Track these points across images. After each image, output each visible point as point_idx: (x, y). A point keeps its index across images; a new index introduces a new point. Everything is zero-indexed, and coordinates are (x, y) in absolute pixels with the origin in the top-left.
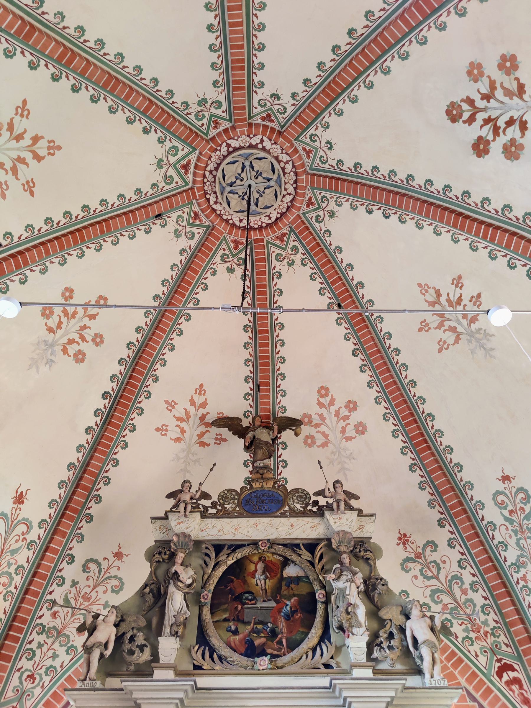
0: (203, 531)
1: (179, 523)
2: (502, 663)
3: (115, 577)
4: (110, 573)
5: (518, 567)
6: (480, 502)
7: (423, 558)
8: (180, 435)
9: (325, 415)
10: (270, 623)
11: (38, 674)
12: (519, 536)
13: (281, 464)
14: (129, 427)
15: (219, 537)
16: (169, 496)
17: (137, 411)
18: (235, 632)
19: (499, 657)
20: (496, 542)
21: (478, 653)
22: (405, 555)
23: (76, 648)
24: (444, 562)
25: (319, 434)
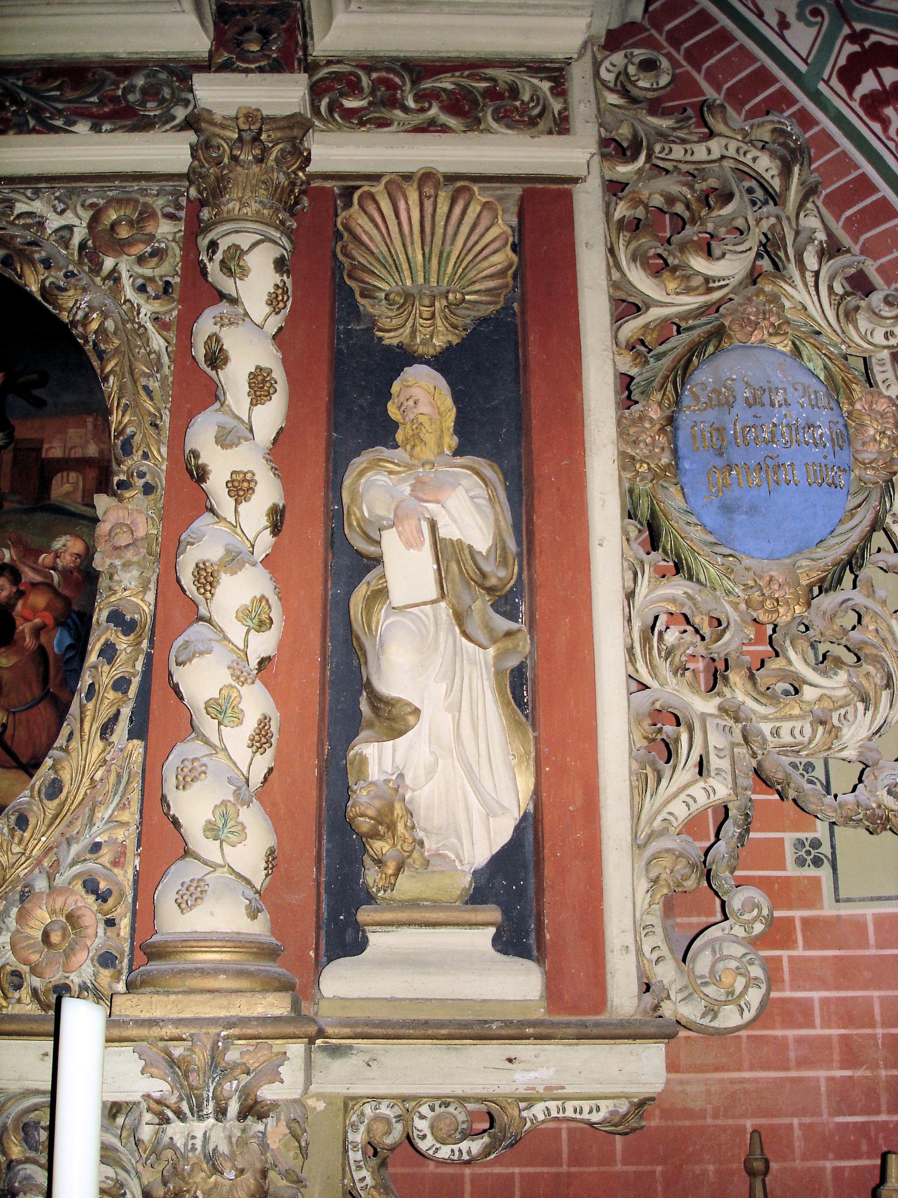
2: (867, 44)
19: (858, 27)
21: (791, 18)
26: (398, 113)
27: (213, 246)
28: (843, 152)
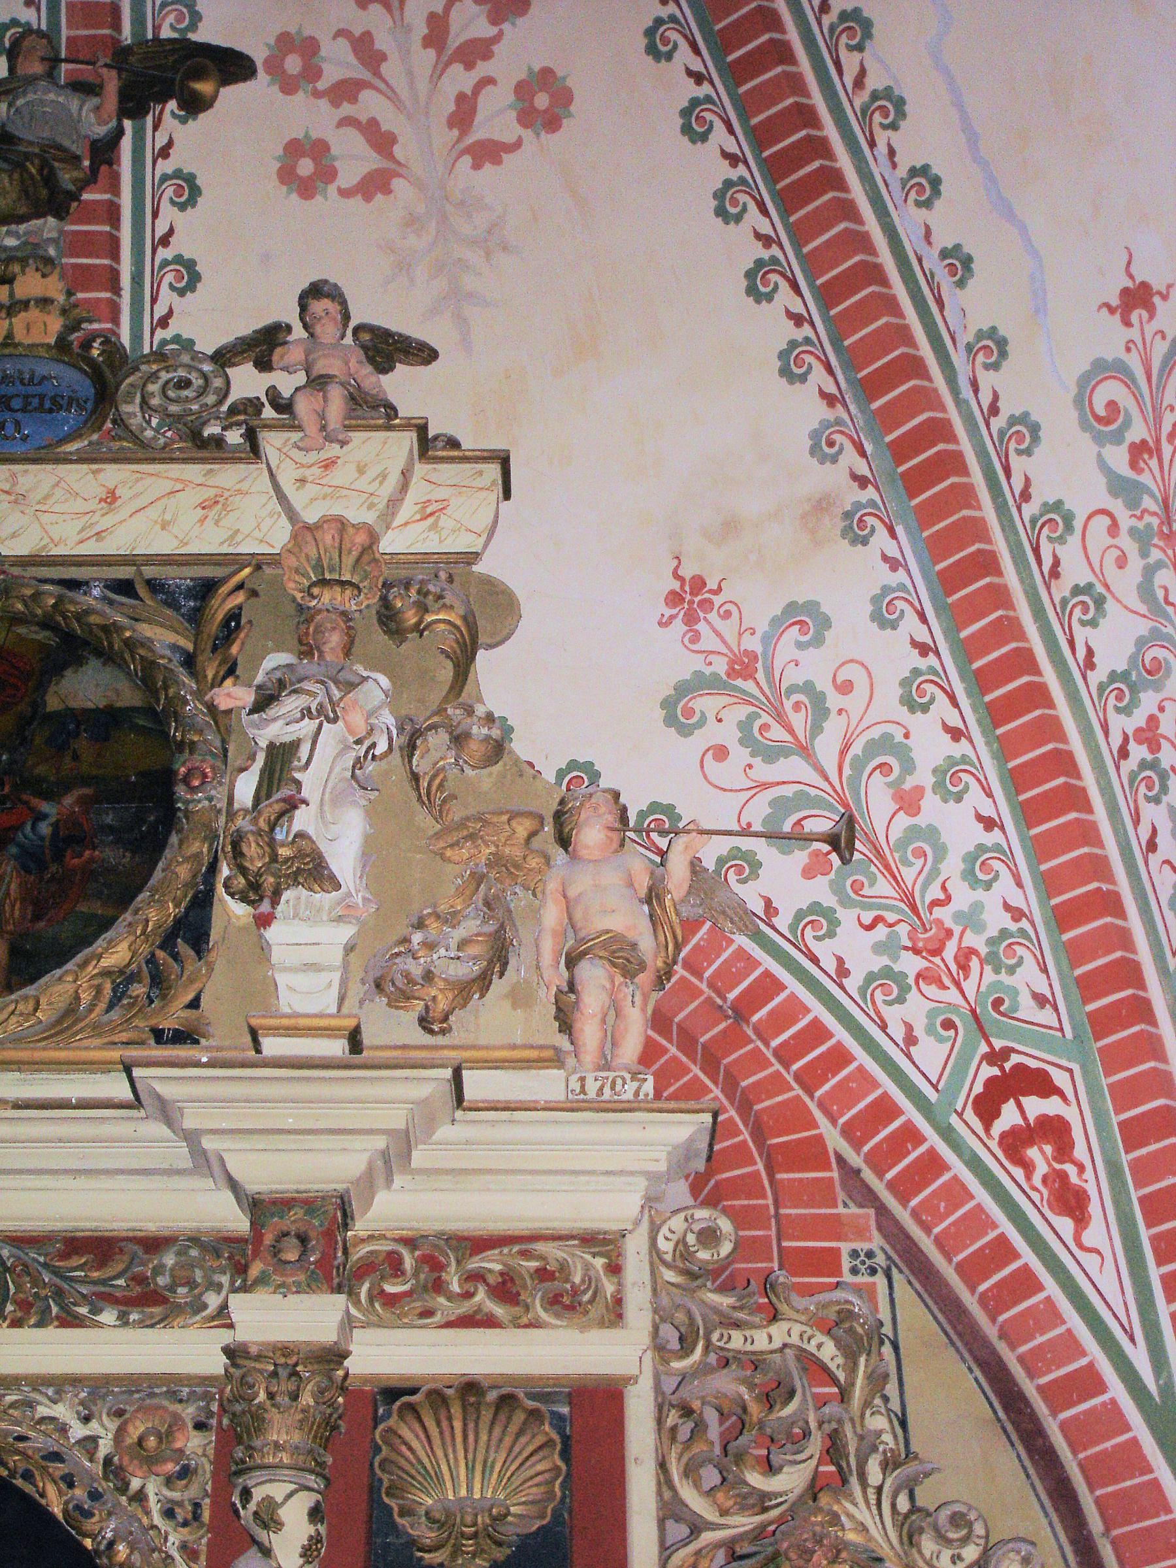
2: (1008, 1066)
5: (1134, 689)
6: (1023, 419)
7: (760, 675)
9: (383, 42)
12: (1156, 555)
13: (169, 278)
19: (998, 1044)
20: (1062, 589)
21: (919, 1032)
22: (689, 665)
24: (846, 688)
25: (351, 133)
26: (442, 1300)
27: (246, 1494)
28: (979, 1205)
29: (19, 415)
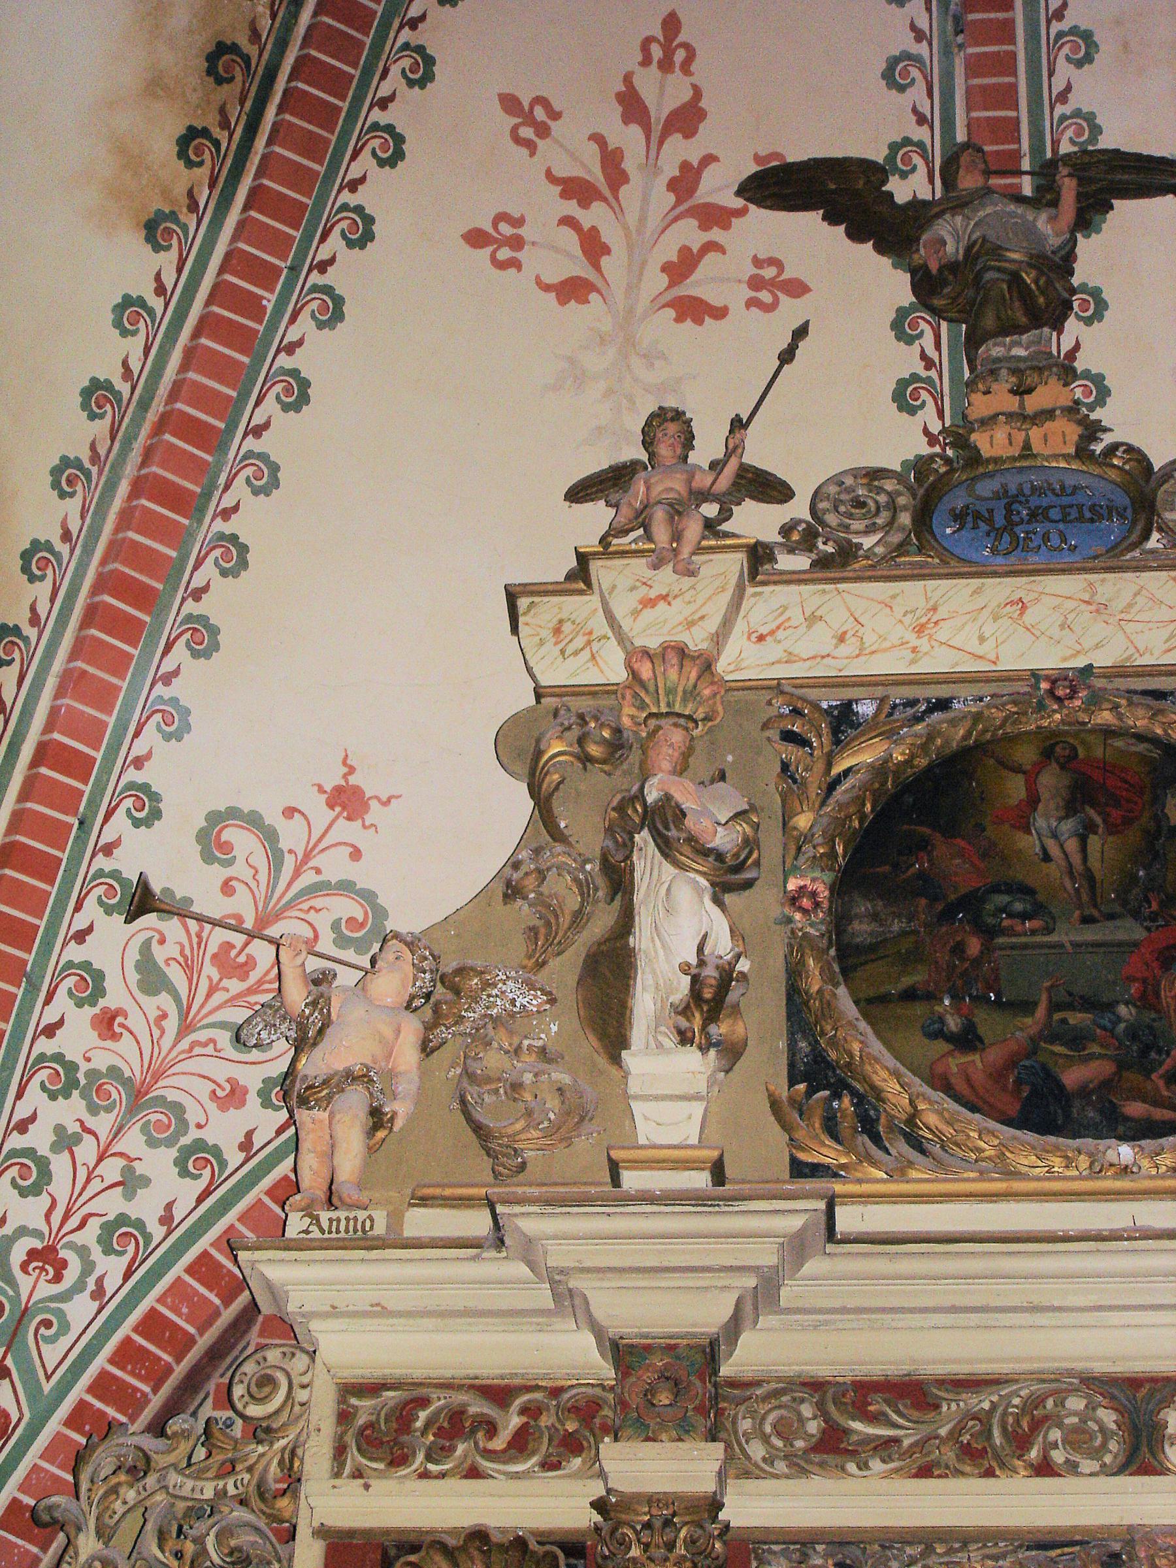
0: (761, 638)
1: (649, 603)
3: (346, 887)
4: (318, 871)
8: (579, 268)
10: (1127, 1003)
11: (71, 1246)
14: (344, 224)
15: (839, 664)
16: (579, 493)
17: (376, 143)
18: (967, 1040)
23: (216, 1151)
29: (1061, 526)
